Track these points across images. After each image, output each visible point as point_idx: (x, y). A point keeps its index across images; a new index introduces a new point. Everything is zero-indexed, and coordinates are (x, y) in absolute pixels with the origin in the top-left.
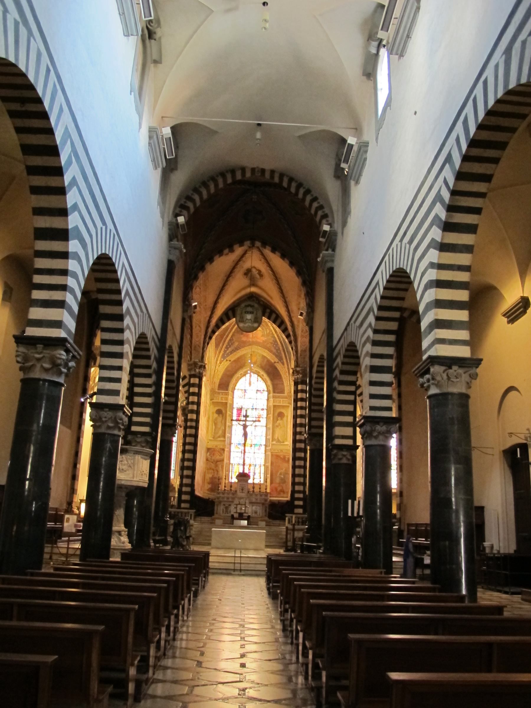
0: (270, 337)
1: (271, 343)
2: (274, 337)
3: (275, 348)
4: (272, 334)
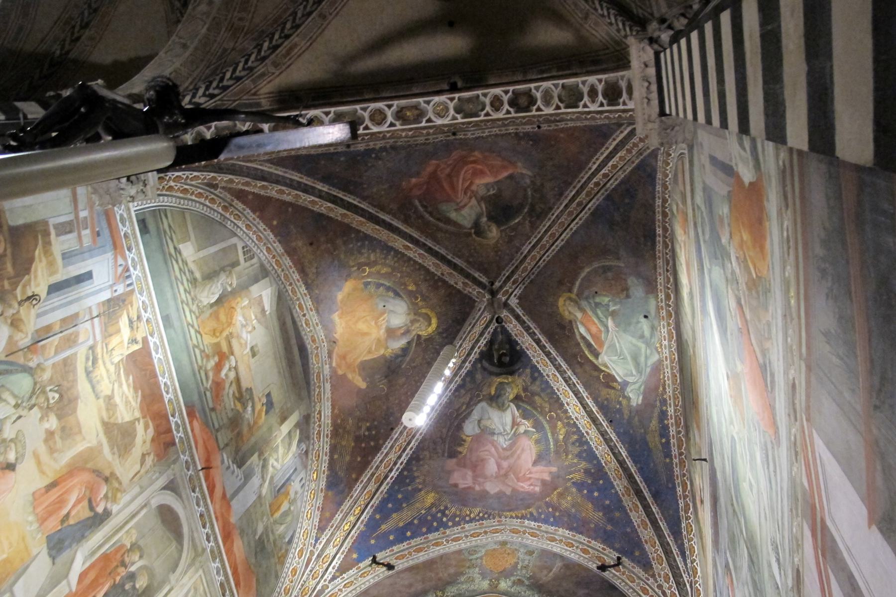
0: (571, 459)
1: (580, 486)
2: (591, 456)
3: (598, 505)
4: (582, 441)
